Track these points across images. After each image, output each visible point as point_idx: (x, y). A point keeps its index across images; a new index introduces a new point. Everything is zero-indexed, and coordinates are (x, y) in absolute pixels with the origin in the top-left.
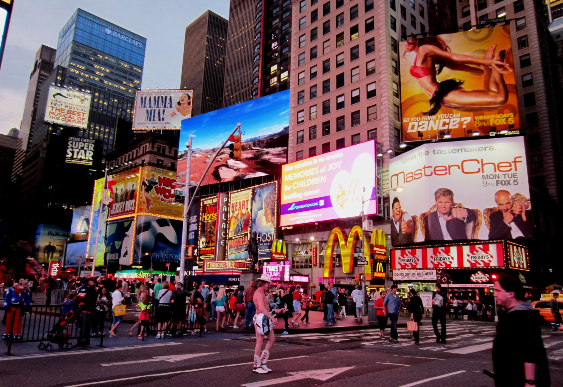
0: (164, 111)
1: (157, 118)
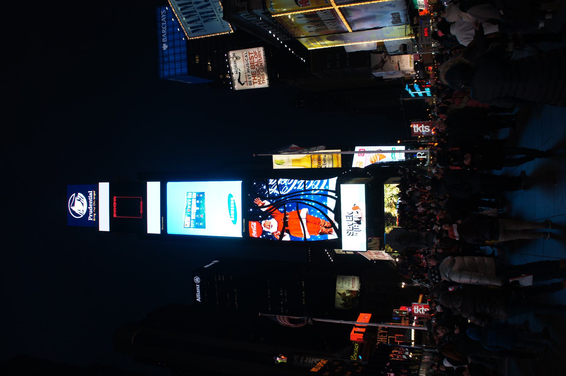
0: (197, 3)
1: (209, 8)
